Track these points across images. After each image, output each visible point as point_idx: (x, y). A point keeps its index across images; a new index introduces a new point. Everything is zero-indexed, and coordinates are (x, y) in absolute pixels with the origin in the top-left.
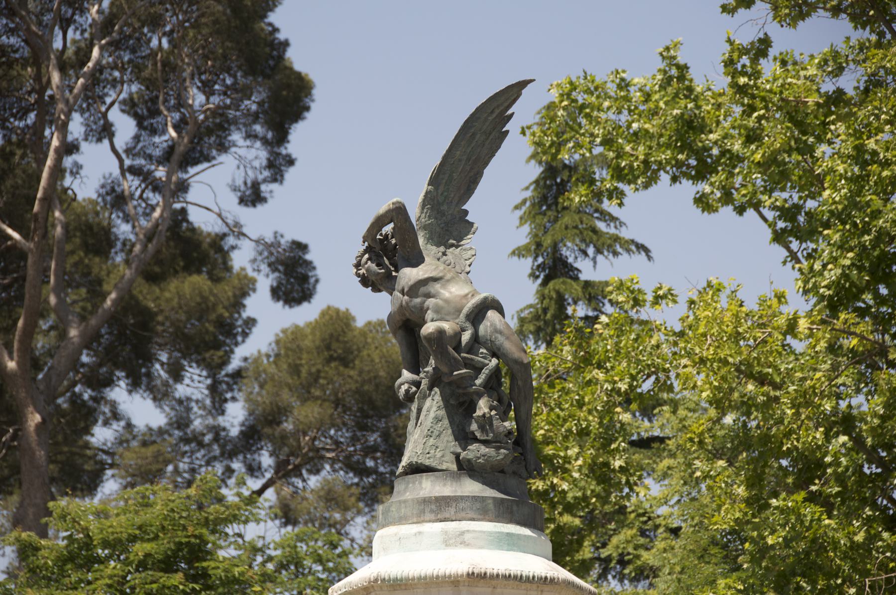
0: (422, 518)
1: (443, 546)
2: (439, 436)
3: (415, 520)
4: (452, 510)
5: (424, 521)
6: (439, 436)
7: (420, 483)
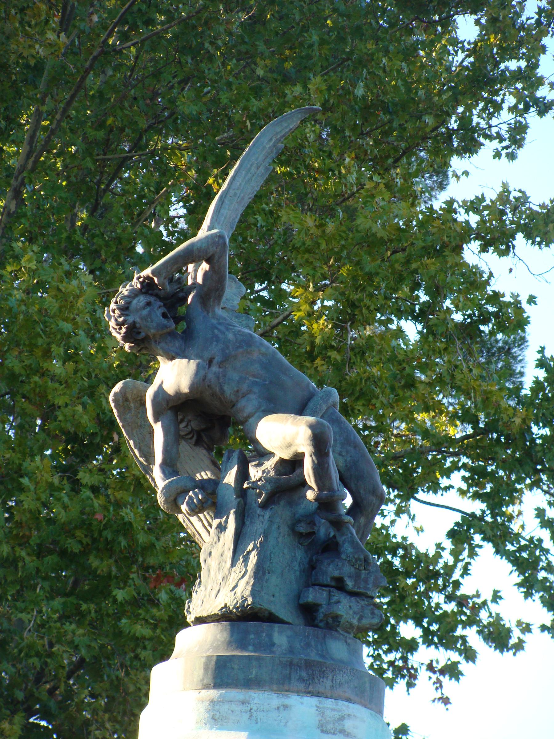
0: (286, 687)
1: (319, 731)
4: (328, 683)
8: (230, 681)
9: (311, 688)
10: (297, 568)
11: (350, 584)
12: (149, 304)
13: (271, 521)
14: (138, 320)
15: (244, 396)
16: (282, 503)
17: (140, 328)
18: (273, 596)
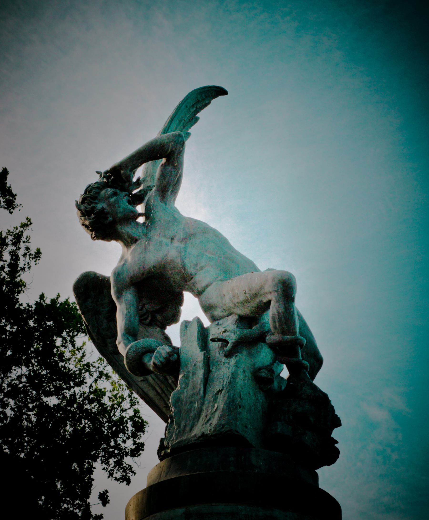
10: (260, 408)
12: (115, 194)
13: (237, 366)
15: (202, 268)
16: (245, 353)
17: (108, 213)
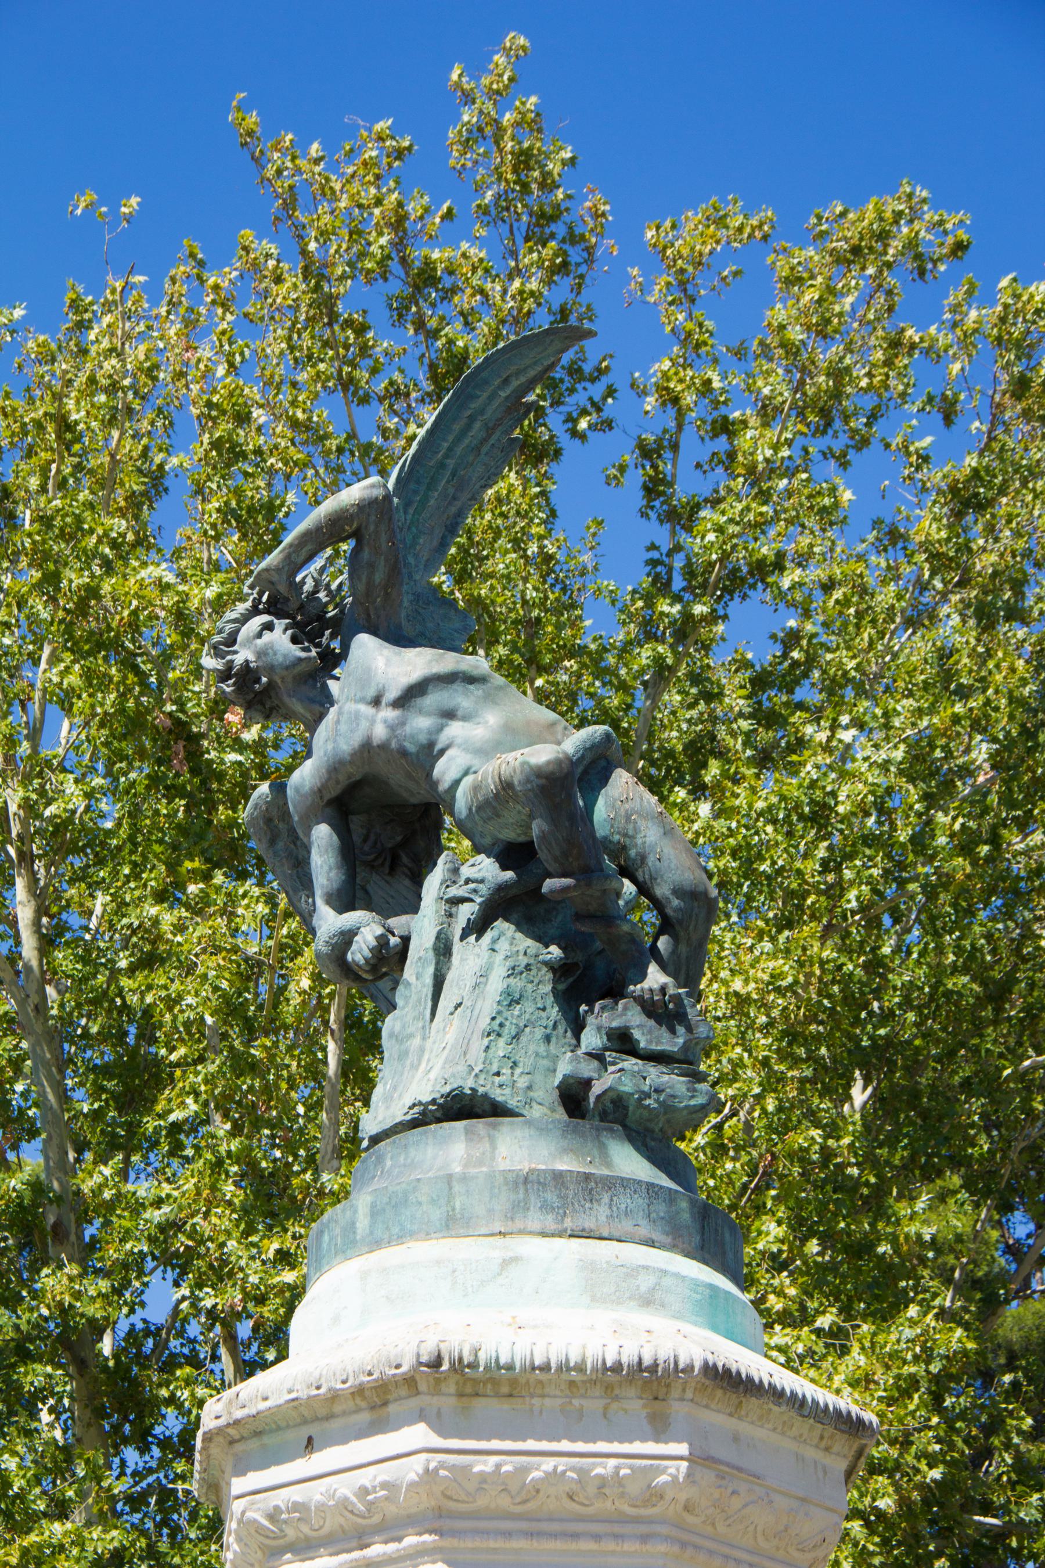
0: (519, 1224)
2: (516, 1037)
3: (498, 1227)
4: (602, 1211)
5: (522, 1232)
6: (516, 1037)
7: (492, 1139)
8: (415, 1227)
9: (568, 1223)
11: (642, 1039)
14: (251, 657)
15: (442, 752)
18: (498, 1074)
